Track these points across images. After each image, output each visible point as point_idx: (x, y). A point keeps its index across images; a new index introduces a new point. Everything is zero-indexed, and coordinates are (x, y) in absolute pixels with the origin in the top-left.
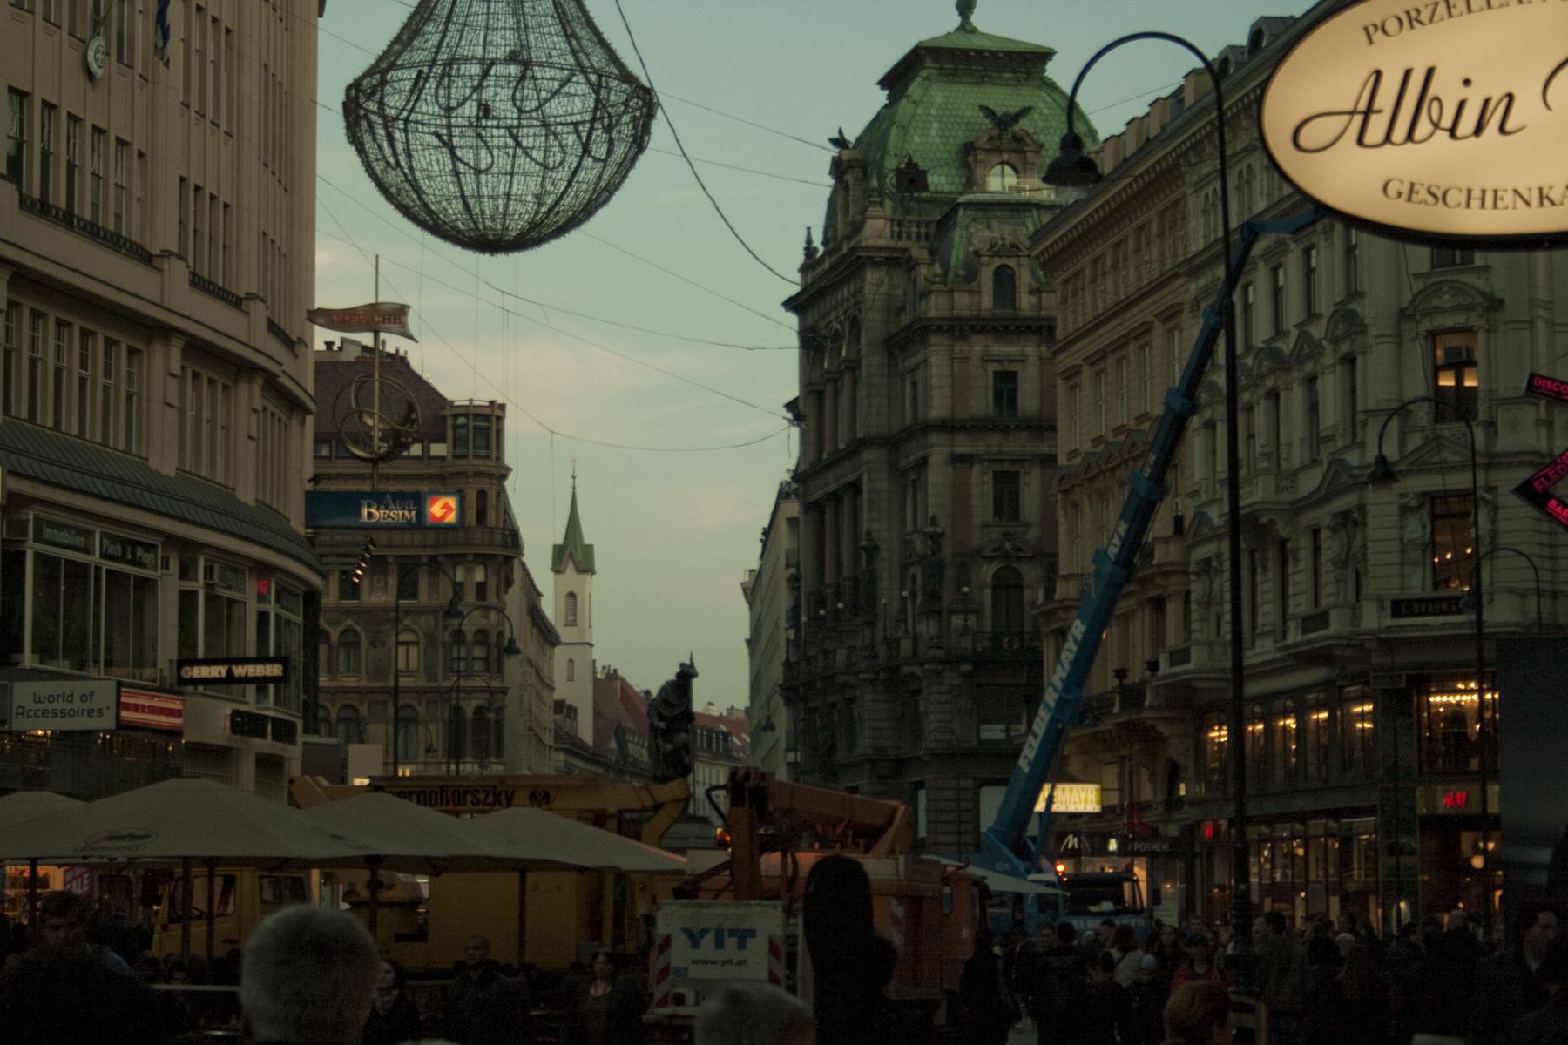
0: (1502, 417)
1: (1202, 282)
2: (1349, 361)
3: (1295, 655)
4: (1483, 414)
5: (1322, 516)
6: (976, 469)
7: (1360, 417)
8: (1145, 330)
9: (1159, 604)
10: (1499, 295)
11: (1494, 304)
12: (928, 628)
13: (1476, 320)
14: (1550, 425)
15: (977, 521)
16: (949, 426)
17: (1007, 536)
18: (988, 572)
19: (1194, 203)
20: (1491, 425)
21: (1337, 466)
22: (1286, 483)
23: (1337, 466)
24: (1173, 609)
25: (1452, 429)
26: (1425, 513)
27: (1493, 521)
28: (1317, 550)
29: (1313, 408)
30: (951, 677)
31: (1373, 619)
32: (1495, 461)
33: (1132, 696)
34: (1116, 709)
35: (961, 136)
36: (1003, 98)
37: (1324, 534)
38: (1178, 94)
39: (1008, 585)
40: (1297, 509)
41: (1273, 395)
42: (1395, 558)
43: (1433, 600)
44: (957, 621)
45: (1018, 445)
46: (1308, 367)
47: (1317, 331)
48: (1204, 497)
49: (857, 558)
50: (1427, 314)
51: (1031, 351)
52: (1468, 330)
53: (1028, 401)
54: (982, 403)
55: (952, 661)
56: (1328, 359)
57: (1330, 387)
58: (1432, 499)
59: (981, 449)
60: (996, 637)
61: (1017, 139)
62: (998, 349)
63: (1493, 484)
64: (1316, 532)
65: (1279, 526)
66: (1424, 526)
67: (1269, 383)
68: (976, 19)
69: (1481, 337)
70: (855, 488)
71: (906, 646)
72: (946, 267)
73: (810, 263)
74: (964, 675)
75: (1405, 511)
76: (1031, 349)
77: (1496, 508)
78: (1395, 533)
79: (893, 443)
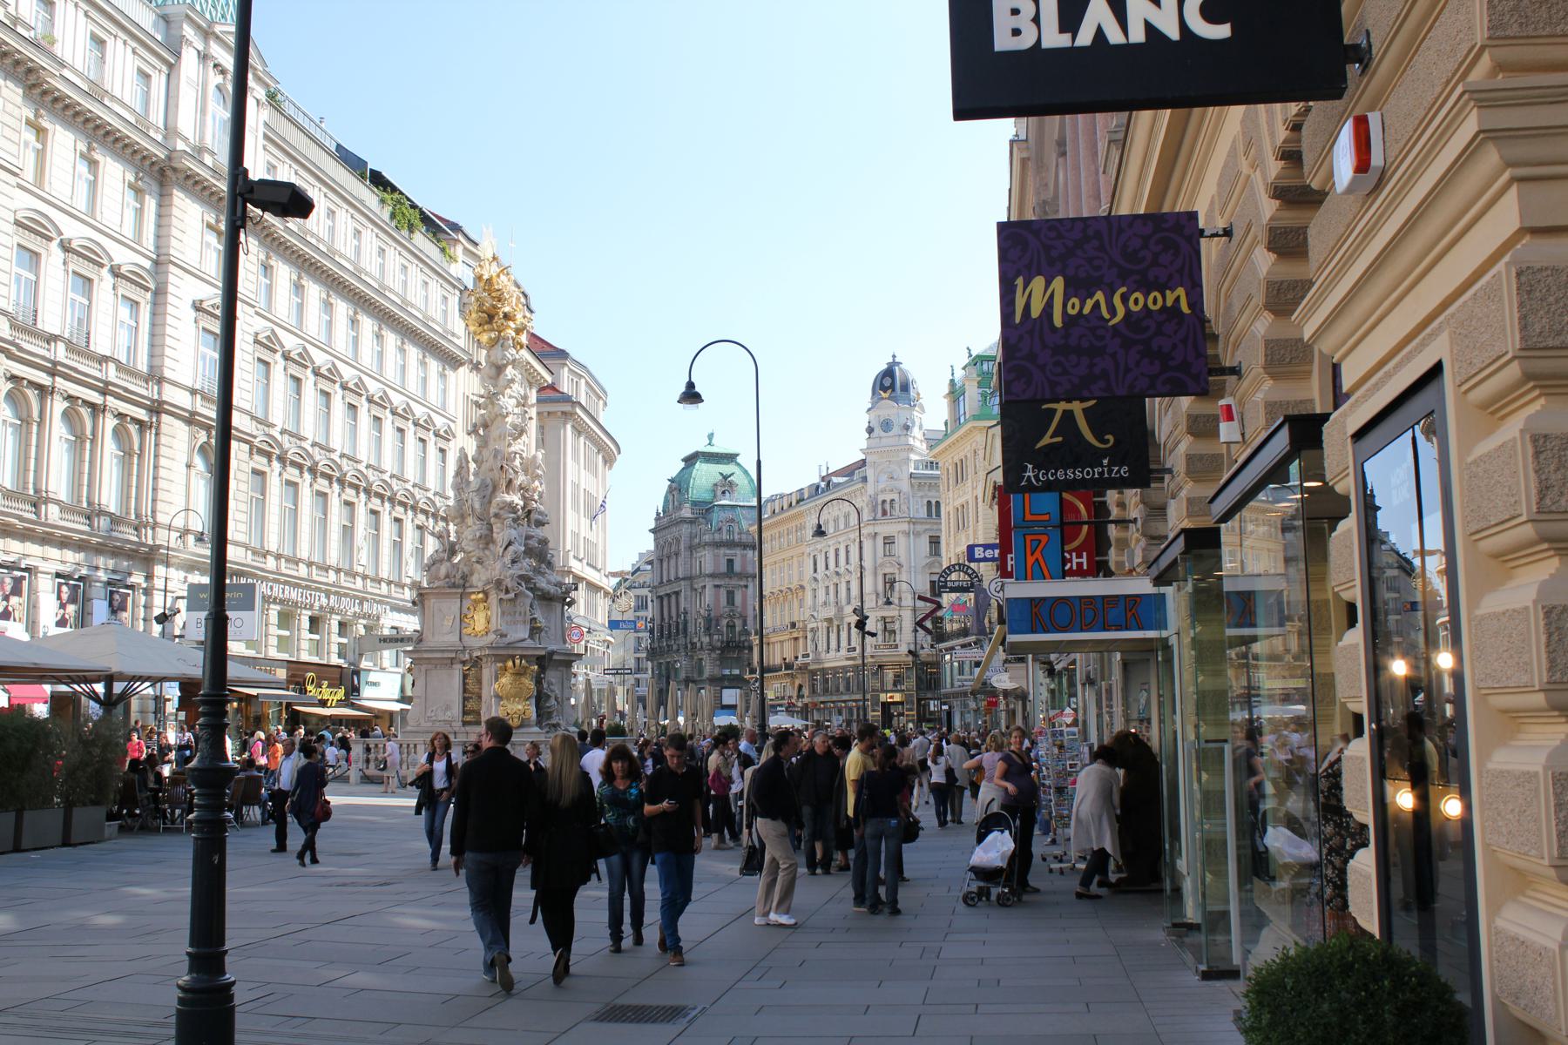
12: (706, 640)
16: (712, 576)
18: (724, 622)
33: (789, 666)
35: (714, 481)
36: (726, 469)
39: (731, 627)
45: (734, 582)
47: (851, 568)
49: (678, 616)
53: (737, 568)
54: (723, 568)
55: (713, 649)
58: (884, 618)
70: (677, 593)
73: (658, 518)
76: (738, 551)
79: (690, 578)
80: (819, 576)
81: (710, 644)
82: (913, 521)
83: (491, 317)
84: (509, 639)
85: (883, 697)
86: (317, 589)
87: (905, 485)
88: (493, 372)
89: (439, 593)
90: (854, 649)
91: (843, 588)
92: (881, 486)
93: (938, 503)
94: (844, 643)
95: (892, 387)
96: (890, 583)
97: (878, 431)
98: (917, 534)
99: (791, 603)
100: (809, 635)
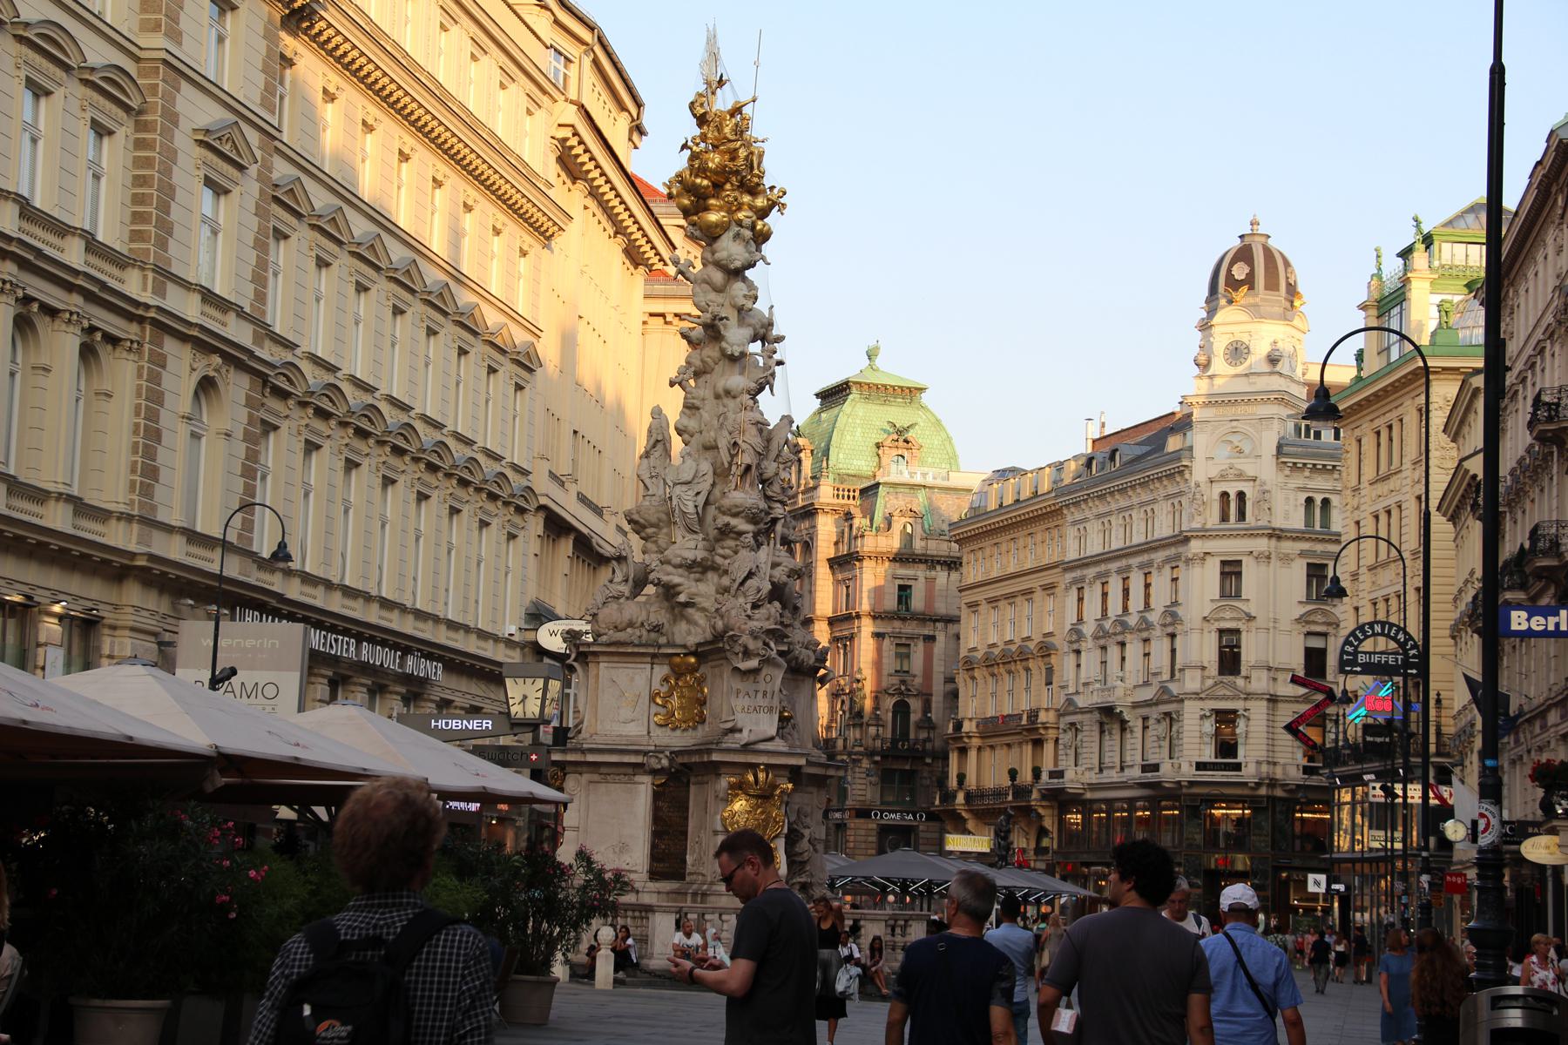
0: (1254, 674)
1: (1074, 575)
2: (1173, 636)
4: (1243, 673)
5: (1154, 713)
6: (887, 641)
7: (1177, 667)
8: (1029, 592)
9: (1038, 743)
11: (1251, 618)
12: (853, 734)
14: (1275, 679)
15: (885, 672)
17: (903, 682)
18: (889, 703)
19: (1071, 532)
21: (1164, 690)
23: (1164, 690)
24: (1049, 748)
25: (1227, 679)
28: (1145, 728)
30: (866, 763)
31: (1188, 772)
32: (1248, 696)
33: (1021, 792)
34: (1010, 798)
36: (899, 414)
37: (1151, 722)
38: (1059, 466)
40: (1136, 705)
41: (1123, 644)
44: (872, 730)
45: (911, 628)
46: (1145, 635)
47: (1154, 617)
48: (1071, 690)
50: (1217, 620)
51: (920, 572)
52: (1237, 632)
53: (917, 603)
54: (891, 603)
56: (1158, 632)
57: (1160, 648)
58: (1218, 712)
59: (889, 630)
60: (894, 741)
61: (906, 441)
62: (902, 571)
64: (1145, 719)
67: (1120, 638)
68: (878, 362)
69: (1244, 635)
71: (840, 743)
72: (872, 520)
74: (876, 763)
75: (1203, 717)
80: (1089, 629)
81: (859, 742)
82: (1277, 535)
83: (718, 187)
84: (744, 737)
85: (1214, 861)
86: (346, 632)
87: (1265, 468)
88: (718, 277)
89: (621, 652)
90: (1155, 768)
93: (1326, 502)
94: (1134, 757)
95: (1250, 281)
97: (1219, 365)
98: (1286, 559)
99: (1027, 669)
100: (1065, 738)
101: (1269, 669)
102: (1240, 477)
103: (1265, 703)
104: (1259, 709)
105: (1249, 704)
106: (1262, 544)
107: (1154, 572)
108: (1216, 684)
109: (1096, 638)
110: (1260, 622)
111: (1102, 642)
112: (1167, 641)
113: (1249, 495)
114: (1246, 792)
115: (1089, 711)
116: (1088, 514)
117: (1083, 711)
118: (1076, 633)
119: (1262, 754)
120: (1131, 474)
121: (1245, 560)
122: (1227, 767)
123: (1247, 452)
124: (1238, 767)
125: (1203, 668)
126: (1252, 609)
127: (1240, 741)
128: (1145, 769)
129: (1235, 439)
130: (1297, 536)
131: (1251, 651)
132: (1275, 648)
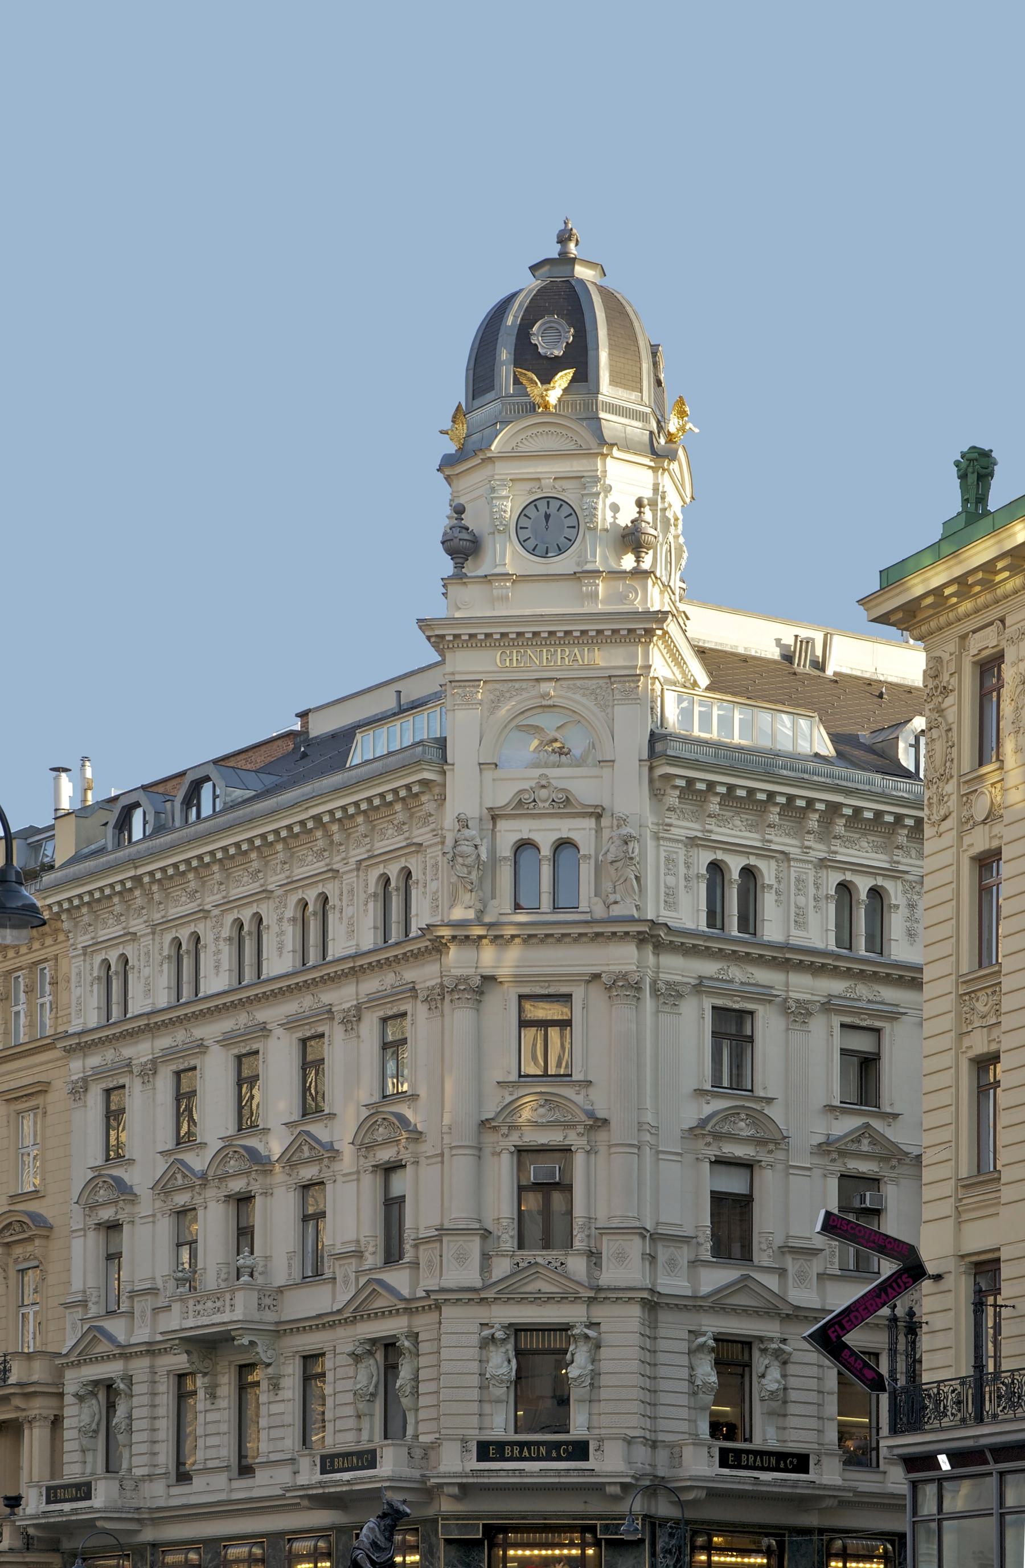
0: (608, 1247)
1: (94, 1060)
3: (310, 1497)
4: (578, 1244)
10: (601, 1114)
11: (598, 1123)
13: (573, 1139)
20: (594, 1256)
22: (267, 1301)
26: (510, 1346)
27: (593, 1361)
29: (312, 1219)
32: (599, 1295)
40: (280, 1331)
42: (475, 1394)
43: (521, 1444)
46: (308, 1173)
63: (595, 1320)
65: (259, 1349)
66: (509, 1361)
67: (237, 1185)
69: (579, 1160)
77: (598, 1347)
78: (474, 1367)
82: (653, 937)
91: (277, 1216)
92: (525, 779)
96: (545, 1188)
101: (642, 1232)
102: (565, 805)
103: (635, 1311)
104: (622, 1324)
105: (600, 1313)
106: (623, 957)
107: (337, 1033)
108: (517, 1270)
109: (163, 1188)
110: (618, 1132)
111: (182, 1199)
112: (370, 1185)
113: (587, 846)
114: (596, 1506)
115: (151, 1350)
116: (137, 925)
117: (125, 1353)
118: (109, 1185)
119: (633, 1424)
120: (250, 821)
121: (578, 993)
122: (554, 1451)
123: (577, 752)
124: (580, 1450)
125: (486, 1234)
126: (601, 1102)
127: (575, 1394)
128: (329, 1463)
129: (548, 722)
130: (689, 947)
131: (598, 1191)
132: (642, 1191)
